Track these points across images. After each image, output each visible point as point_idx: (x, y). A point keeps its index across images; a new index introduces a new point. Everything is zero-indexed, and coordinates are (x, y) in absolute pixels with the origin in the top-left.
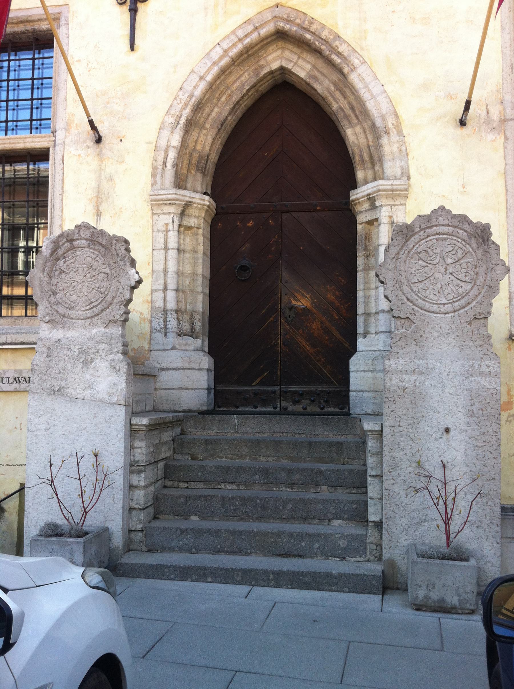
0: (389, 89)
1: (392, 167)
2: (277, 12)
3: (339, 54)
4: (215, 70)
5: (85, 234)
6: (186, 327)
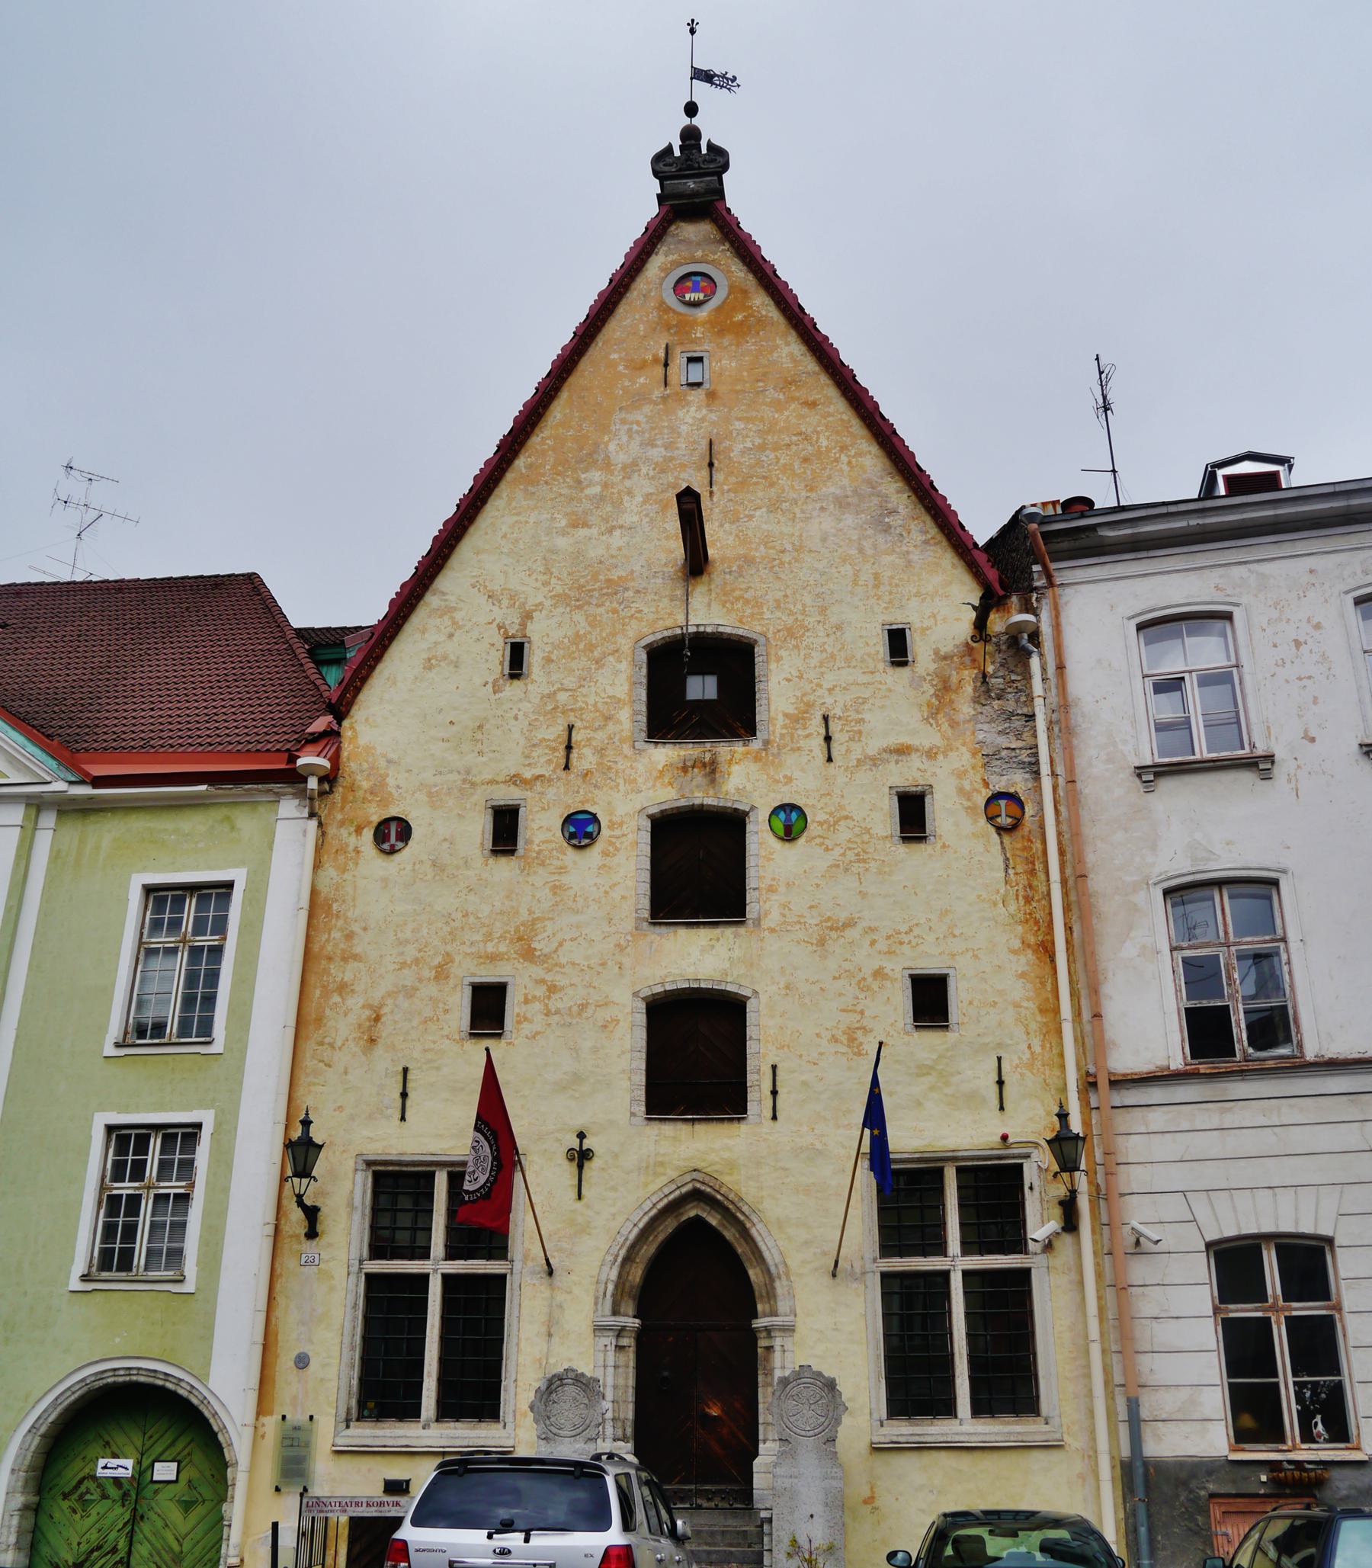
0: (780, 1243)
1: (782, 1306)
2: (695, 1175)
3: (743, 1213)
4: (646, 1219)
5: (571, 1375)
6: (620, 1433)
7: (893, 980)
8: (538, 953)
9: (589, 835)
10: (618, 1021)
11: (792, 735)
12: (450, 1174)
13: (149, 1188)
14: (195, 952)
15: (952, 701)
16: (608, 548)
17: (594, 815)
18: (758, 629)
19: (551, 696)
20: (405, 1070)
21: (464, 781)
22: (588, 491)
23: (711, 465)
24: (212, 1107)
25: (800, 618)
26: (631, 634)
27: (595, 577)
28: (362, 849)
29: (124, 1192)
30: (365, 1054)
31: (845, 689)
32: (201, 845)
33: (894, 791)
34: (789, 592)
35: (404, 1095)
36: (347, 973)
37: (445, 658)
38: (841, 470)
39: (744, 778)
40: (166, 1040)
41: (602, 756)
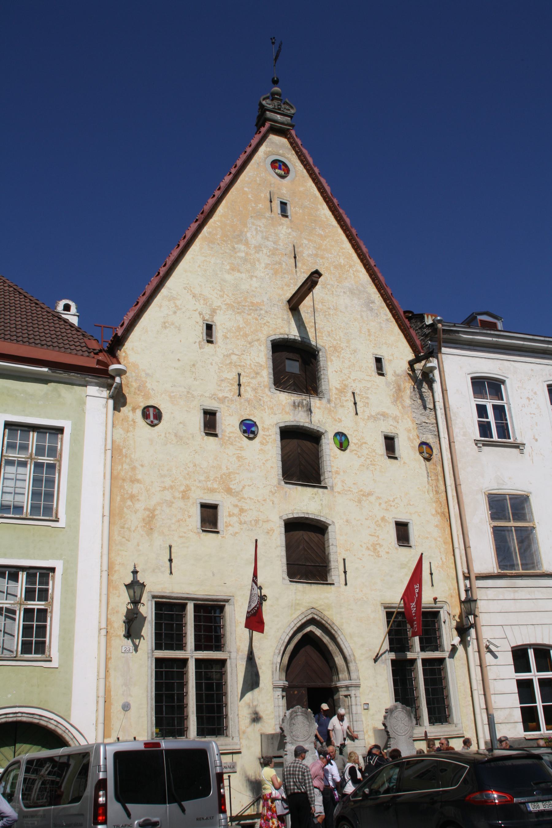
0: (351, 645)
1: (353, 675)
7: (389, 523)
8: (233, 491)
9: (253, 432)
10: (274, 530)
11: (340, 399)
12: (196, 606)
13: (21, 604)
14: (38, 466)
15: (402, 397)
16: (251, 286)
17: (255, 423)
18: (322, 344)
19: (228, 356)
20: (170, 547)
21: (188, 392)
22: (239, 254)
23: (295, 257)
24: (60, 559)
25: (339, 343)
26: (265, 333)
27: (245, 299)
28: (137, 421)
29: (36, 607)
30: (148, 535)
31: (360, 381)
32: (41, 403)
33: (383, 434)
34: (333, 329)
35: (171, 560)
36: (135, 489)
37: (173, 324)
38: (351, 276)
39: (322, 416)
40: (24, 516)
41: (256, 393)
